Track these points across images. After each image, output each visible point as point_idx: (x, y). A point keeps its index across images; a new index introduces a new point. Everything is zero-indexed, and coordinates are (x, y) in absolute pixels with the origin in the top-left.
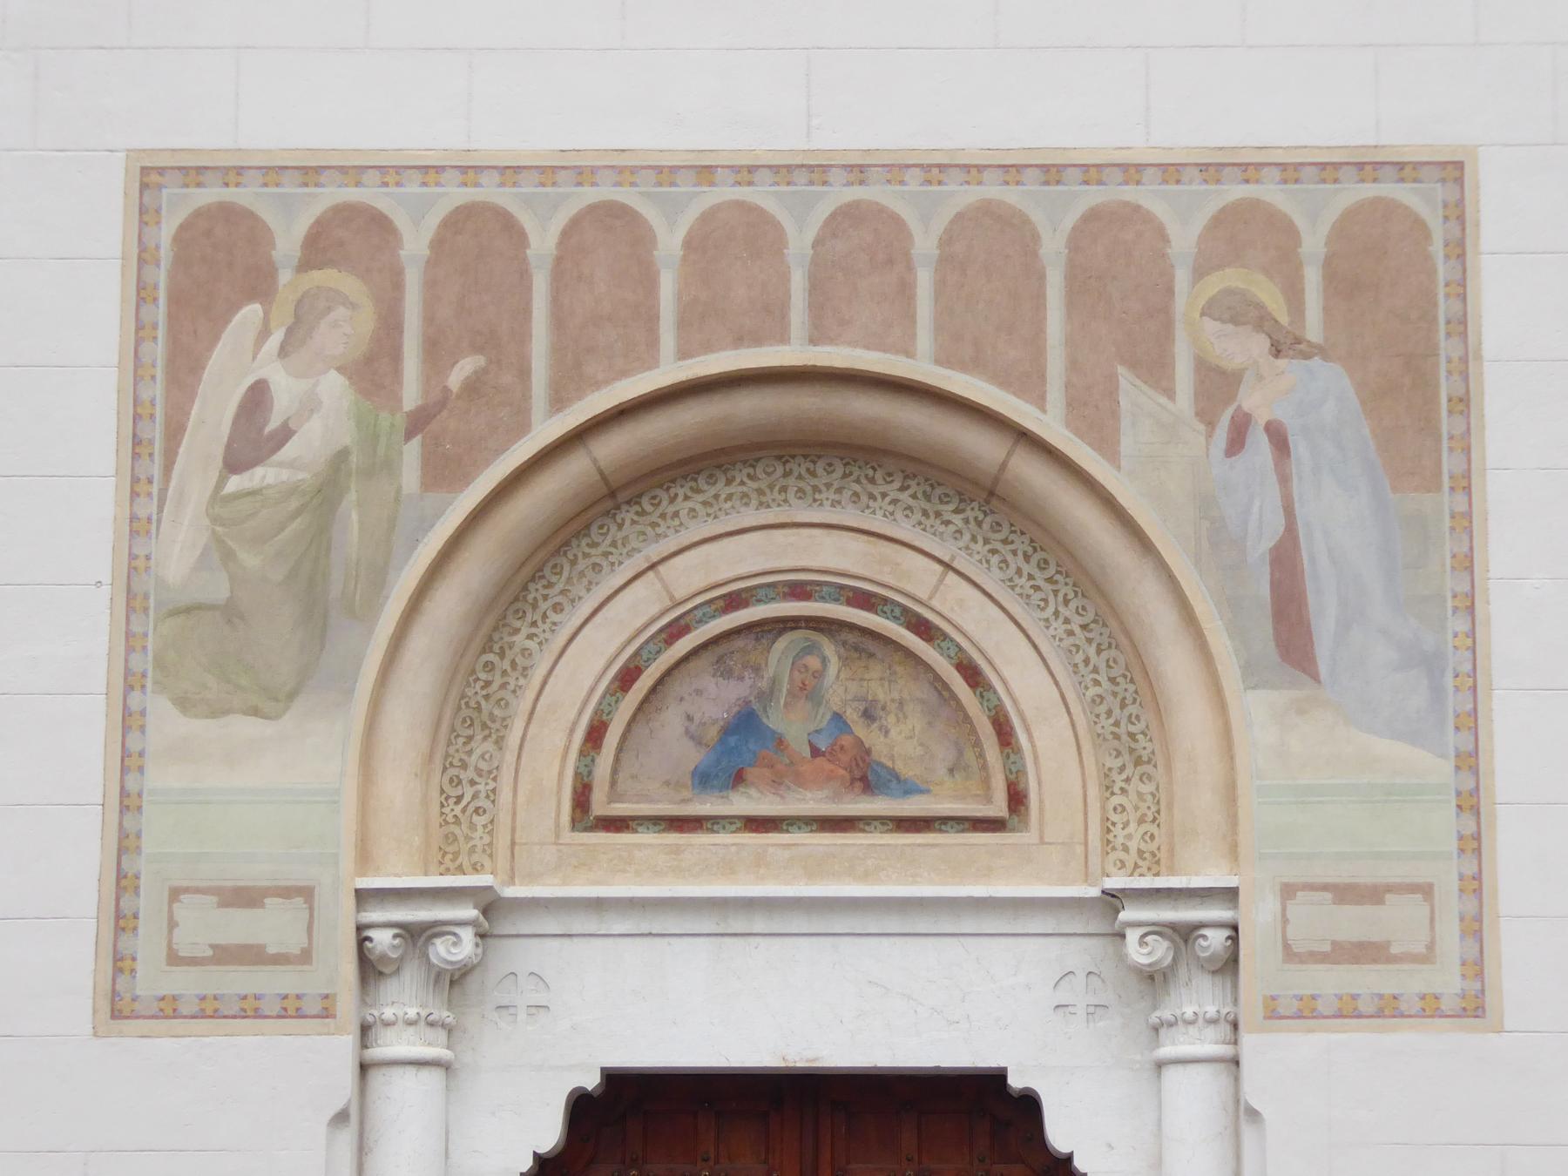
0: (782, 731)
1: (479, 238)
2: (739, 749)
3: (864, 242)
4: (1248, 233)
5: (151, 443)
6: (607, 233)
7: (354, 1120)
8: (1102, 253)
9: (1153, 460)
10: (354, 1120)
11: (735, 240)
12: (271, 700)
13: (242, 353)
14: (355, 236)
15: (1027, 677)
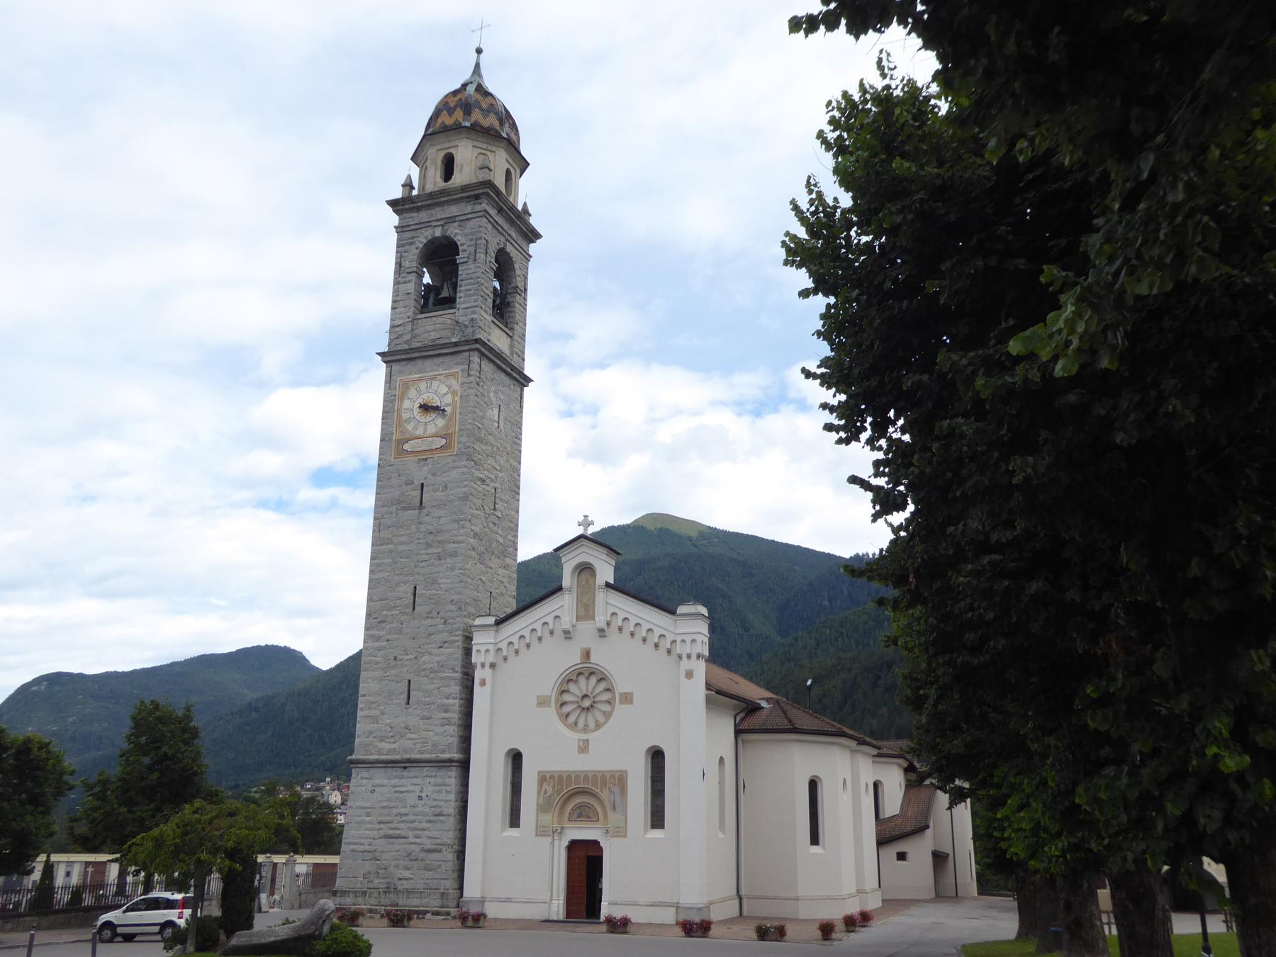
0: (584, 814)
1: (560, 777)
2: (580, 815)
3: (586, 777)
4: (612, 776)
5: (539, 793)
6: (569, 777)
7: (552, 843)
8: (602, 778)
9: (605, 796)
10: (552, 843)
11: (578, 777)
12: (546, 812)
13: (545, 786)
14: (552, 777)
15: (599, 810)
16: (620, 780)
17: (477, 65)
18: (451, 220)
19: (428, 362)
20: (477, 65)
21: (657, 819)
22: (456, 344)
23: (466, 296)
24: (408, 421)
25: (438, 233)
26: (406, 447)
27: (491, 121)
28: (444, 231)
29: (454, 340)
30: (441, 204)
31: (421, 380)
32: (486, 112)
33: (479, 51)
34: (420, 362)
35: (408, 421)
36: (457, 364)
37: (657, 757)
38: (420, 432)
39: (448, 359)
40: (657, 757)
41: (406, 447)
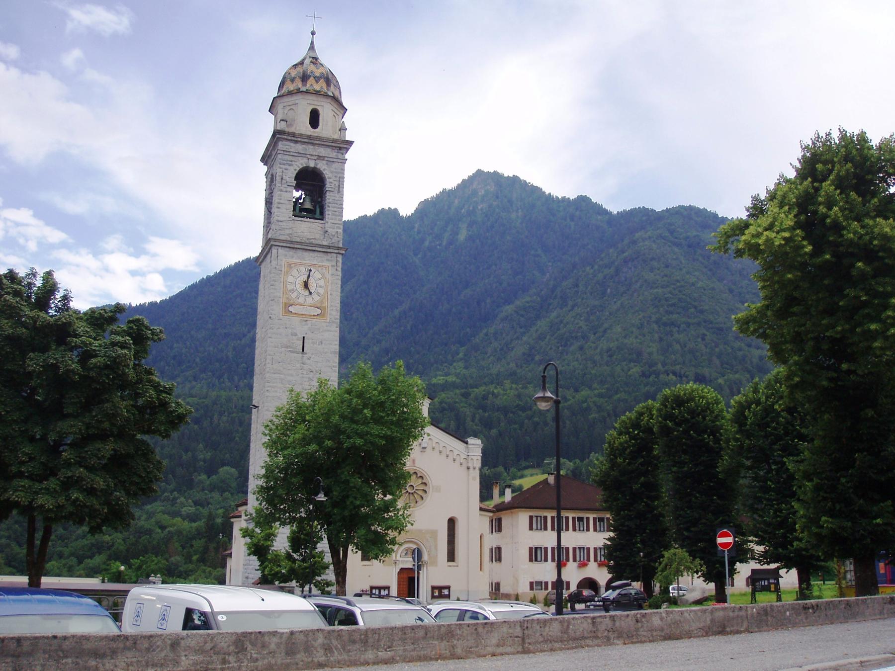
16: (434, 534)
17: (312, 43)
18: (320, 158)
19: (306, 254)
20: (312, 43)
21: (451, 557)
22: (329, 247)
23: (333, 215)
24: (292, 291)
25: (312, 164)
26: (291, 309)
27: (320, 86)
28: (316, 164)
29: (325, 243)
30: (313, 144)
31: (301, 264)
32: (317, 79)
33: (313, 33)
34: (300, 253)
35: (292, 291)
36: (328, 260)
37: (452, 522)
38: (301, 300)
39: (321, 254)
40: (452, 522)
41: (291, 309)
